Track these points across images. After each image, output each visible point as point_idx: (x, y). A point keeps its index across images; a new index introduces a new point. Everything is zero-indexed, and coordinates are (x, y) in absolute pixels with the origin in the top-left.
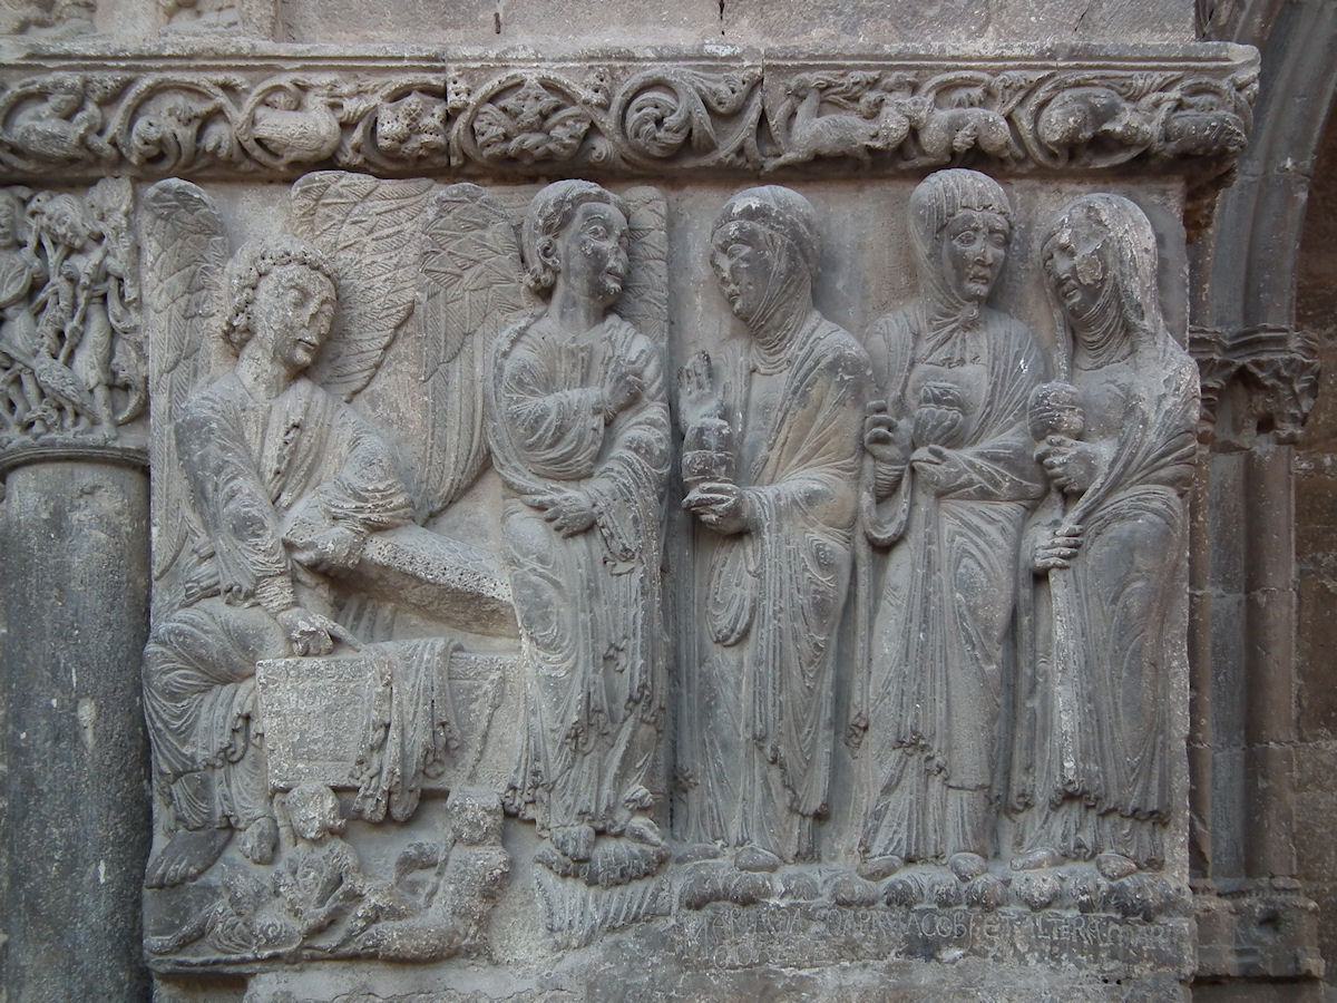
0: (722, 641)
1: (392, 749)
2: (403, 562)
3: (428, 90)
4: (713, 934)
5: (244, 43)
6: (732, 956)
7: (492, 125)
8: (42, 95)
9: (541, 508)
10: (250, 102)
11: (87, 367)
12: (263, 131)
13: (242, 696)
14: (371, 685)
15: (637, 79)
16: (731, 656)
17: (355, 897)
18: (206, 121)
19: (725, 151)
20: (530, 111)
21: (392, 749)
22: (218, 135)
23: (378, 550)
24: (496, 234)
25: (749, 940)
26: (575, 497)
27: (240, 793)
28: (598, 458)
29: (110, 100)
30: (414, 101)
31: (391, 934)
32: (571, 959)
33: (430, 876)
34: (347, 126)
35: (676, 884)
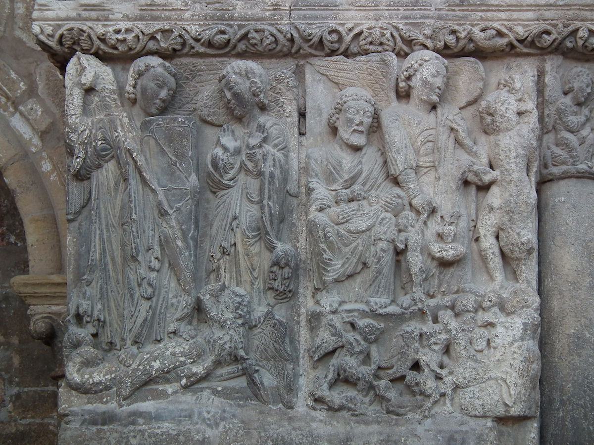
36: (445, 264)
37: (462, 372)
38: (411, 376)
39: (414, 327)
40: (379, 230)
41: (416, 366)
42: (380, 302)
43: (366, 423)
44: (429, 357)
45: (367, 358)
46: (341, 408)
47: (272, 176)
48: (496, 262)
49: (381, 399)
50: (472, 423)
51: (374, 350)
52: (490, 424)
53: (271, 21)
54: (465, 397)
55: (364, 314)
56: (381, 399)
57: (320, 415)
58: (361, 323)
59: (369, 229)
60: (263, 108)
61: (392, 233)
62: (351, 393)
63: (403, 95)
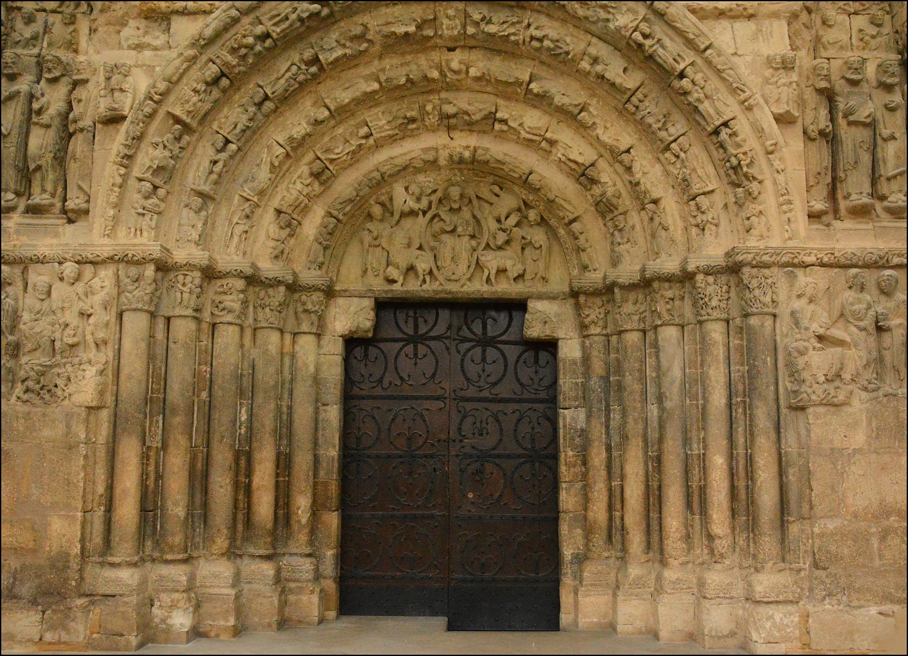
0: (885, 349)
1: (834, 368)
2: (832, 335)
3: (832, 254)
4: (889, 401)
5: (801, 246)
6: (892, 405)
7: (842, 260)
8: (767, 254)
9: (855, 326)
10: (802, 255)
11: (768, 299)
12: (804, 260)
13: (806, 358)
14: (830, 356)
15: (867, 252)
16: (887, 352)
17: (829, 394)
18: (793, 258)
19: (880, 264)
20: (849, 258)
21: (834, 368)
22: (796, 261)
23: (828, 333)
24: (843, 278)
25: (895, 402)
26: (862, 324)
27: (805, 375)
28: (865, 317)
29: (778, 254)
30: (829, 255)
31: (835, 400)
32: (864, 405)
33: (839, 390)
34: (818, 259)
35: (881, 392)
36: (72, 346)
37: (72, 388)
38: (54, 389)
39: (56, 370)
40: (45, 332)
41: (56, 386)
42: (45, 360)
43: (37, 407)
44: (61, 382)
45: (39, 383)
46: (27, 401)
47: (8, 311)
48: (93, 345)
49: (42, 398)
50: (76, 408)
51: (42, 378)
52: (83, 409)
53: (12, 251)
54: (73, 398)
55: (38, 365)
56: (42, 398)
57: (19, 403)
58: (35, 368)
59: (41, 332)
60: (10, 284)
61: (50, 334)
62: (32, 395)
63: (62, 279)
